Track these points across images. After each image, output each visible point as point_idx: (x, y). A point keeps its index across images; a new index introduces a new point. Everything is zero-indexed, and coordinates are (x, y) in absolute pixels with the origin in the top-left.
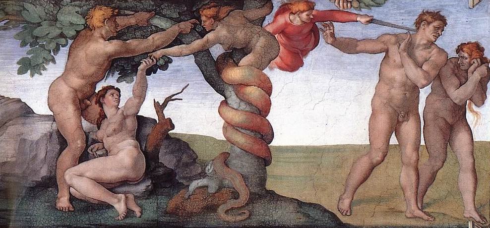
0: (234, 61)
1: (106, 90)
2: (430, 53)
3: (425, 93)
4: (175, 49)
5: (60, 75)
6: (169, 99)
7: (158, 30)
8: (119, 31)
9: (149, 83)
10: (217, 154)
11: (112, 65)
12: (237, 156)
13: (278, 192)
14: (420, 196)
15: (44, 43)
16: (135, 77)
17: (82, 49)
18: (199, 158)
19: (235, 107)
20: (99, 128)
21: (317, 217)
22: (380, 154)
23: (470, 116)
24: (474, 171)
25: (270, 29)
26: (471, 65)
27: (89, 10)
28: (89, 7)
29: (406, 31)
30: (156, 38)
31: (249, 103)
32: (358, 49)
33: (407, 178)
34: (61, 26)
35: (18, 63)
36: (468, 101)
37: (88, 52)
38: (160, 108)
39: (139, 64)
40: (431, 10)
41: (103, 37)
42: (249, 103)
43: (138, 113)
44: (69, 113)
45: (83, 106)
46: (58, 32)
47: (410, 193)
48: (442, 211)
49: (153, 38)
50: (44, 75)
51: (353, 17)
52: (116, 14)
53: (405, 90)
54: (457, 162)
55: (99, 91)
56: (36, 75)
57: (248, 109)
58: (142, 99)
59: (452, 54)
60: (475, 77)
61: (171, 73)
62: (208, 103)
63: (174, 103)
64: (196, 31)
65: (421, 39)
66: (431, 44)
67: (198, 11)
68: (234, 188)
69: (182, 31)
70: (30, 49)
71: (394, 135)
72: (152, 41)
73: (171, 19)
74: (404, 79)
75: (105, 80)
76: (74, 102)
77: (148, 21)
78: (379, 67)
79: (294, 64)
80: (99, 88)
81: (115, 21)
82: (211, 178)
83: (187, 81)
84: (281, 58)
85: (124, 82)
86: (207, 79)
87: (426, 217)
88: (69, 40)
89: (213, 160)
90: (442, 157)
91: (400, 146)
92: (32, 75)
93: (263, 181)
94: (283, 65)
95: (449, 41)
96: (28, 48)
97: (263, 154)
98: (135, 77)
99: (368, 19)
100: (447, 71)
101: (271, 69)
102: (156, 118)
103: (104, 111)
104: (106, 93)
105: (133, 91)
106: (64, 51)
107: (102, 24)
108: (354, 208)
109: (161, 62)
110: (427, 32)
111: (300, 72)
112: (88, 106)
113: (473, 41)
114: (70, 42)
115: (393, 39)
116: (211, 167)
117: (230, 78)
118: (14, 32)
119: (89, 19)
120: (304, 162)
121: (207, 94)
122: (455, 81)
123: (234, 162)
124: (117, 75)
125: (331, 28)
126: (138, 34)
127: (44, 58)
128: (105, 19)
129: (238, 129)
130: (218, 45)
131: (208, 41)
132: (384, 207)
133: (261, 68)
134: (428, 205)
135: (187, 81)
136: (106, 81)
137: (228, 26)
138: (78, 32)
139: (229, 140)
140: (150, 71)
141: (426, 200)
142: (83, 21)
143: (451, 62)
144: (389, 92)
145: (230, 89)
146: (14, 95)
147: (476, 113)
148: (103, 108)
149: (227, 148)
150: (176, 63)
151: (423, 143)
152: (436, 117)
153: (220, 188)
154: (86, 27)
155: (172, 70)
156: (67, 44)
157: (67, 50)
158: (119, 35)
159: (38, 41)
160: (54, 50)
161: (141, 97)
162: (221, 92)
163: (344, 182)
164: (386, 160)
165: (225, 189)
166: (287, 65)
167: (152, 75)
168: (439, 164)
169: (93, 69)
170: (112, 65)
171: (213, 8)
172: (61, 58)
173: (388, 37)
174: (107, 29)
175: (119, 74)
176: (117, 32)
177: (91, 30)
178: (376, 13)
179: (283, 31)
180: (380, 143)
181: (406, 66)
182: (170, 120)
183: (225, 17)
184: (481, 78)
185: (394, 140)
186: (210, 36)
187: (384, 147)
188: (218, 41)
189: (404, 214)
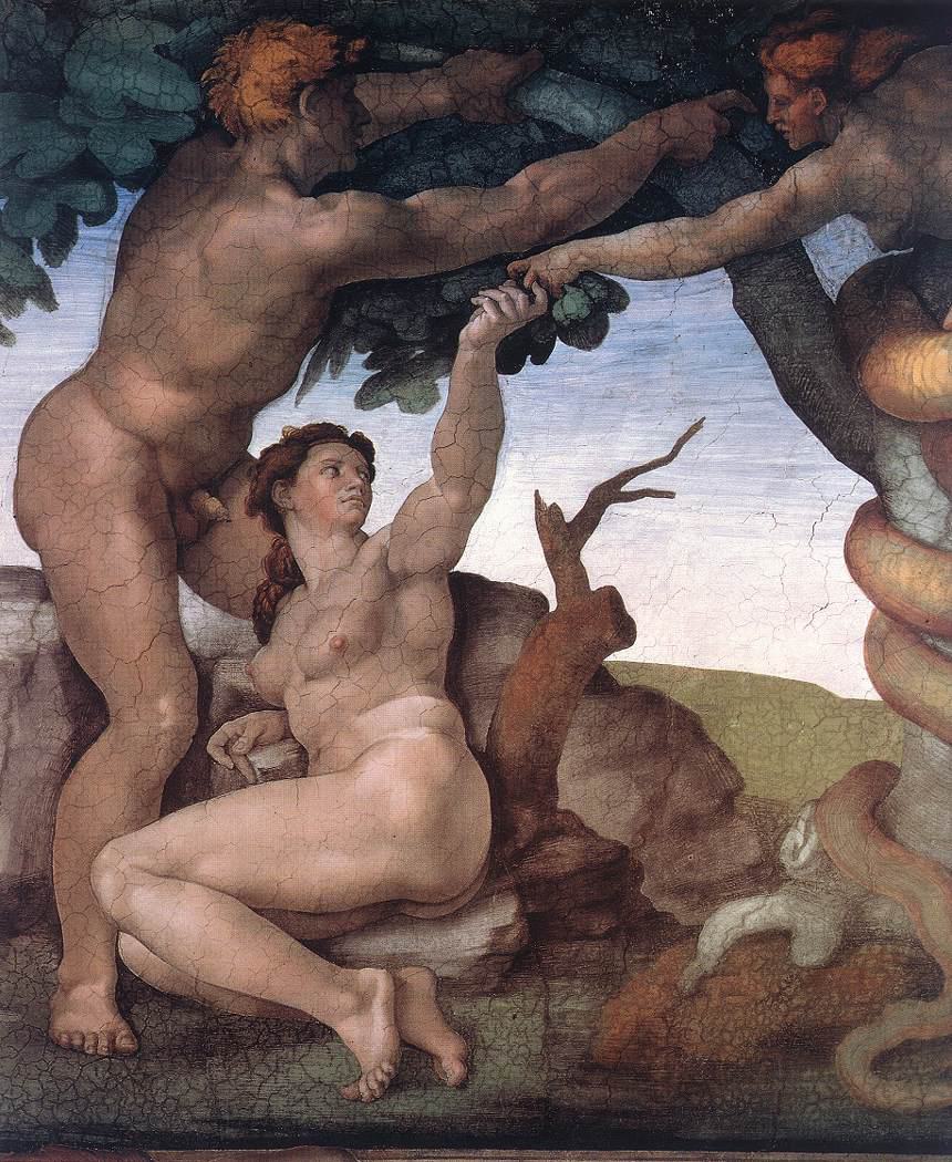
0: (922, 302)
1: (301, 443)
4: (639, 240)
6: (608, 494)
7: (559, 141)
8: (371, 147)
9: (512, 411)
10: (835, 768)
11: (334, 318)
16: (443, 383)
17: (187, 234)
18: (748, 792)
19: (927, 532)
20: (264, 630)
27: (218, 38)
28: (218, 21)
34: (87, 122)
37: (211, 252)
39: (465, 312)
45: (188, 523)
49: (534, 185)
52: (353, 59)
55: (266, 452)
58: (476, 491)
61: (620, 363)
63: (635, 512)
64: (742, 148)
68: (917, 944)
69: (674, 150)
72: (527, 200)
75: (301, 393)
76: (142, 501)
77: (510, 94)
80: (266, 433)
81: (350, 100)
82: (805, 889)
83: (694, 403)
85: (393, 406)
86: (794, 395)
88: (122, 192)
89: (818, 801)
98: (443, 383)
102: (546, 585)
103: (289, 547)
105: (434, 452)
106: (96, 245)
107: (277, 113)
109: (572, 305)
112: (208, 525)
114: (127, 200)
116: (806, 840)
117: (904, 388)
119: (221, 87)
121: (793, 467)
124: (356, 370)
126: (461, 161)
128: (299, 87)
129: (939, 644)
130: (850, 220)
131: (795, 204)
135: (694, 403)
136: (306, 399)
137: (895, 125)
138: (165, 152)
142: (188, 96)
145: (906, 444)
148: (285, 535)
149: (887, 742)
150: (646, 307)
153: (852, 939)
155: (624, 347)
156: (111, 213)
157: (109, 240)
162: (860, 459)
165: (877, 948)
167: (529, 368)
170: (334, 318)
171: (824, 37)
175: (368, 365)
176: (358, 151)
177: (230, 141)
182: (612, 598)
183: (875, 83)
186: (807, 175)
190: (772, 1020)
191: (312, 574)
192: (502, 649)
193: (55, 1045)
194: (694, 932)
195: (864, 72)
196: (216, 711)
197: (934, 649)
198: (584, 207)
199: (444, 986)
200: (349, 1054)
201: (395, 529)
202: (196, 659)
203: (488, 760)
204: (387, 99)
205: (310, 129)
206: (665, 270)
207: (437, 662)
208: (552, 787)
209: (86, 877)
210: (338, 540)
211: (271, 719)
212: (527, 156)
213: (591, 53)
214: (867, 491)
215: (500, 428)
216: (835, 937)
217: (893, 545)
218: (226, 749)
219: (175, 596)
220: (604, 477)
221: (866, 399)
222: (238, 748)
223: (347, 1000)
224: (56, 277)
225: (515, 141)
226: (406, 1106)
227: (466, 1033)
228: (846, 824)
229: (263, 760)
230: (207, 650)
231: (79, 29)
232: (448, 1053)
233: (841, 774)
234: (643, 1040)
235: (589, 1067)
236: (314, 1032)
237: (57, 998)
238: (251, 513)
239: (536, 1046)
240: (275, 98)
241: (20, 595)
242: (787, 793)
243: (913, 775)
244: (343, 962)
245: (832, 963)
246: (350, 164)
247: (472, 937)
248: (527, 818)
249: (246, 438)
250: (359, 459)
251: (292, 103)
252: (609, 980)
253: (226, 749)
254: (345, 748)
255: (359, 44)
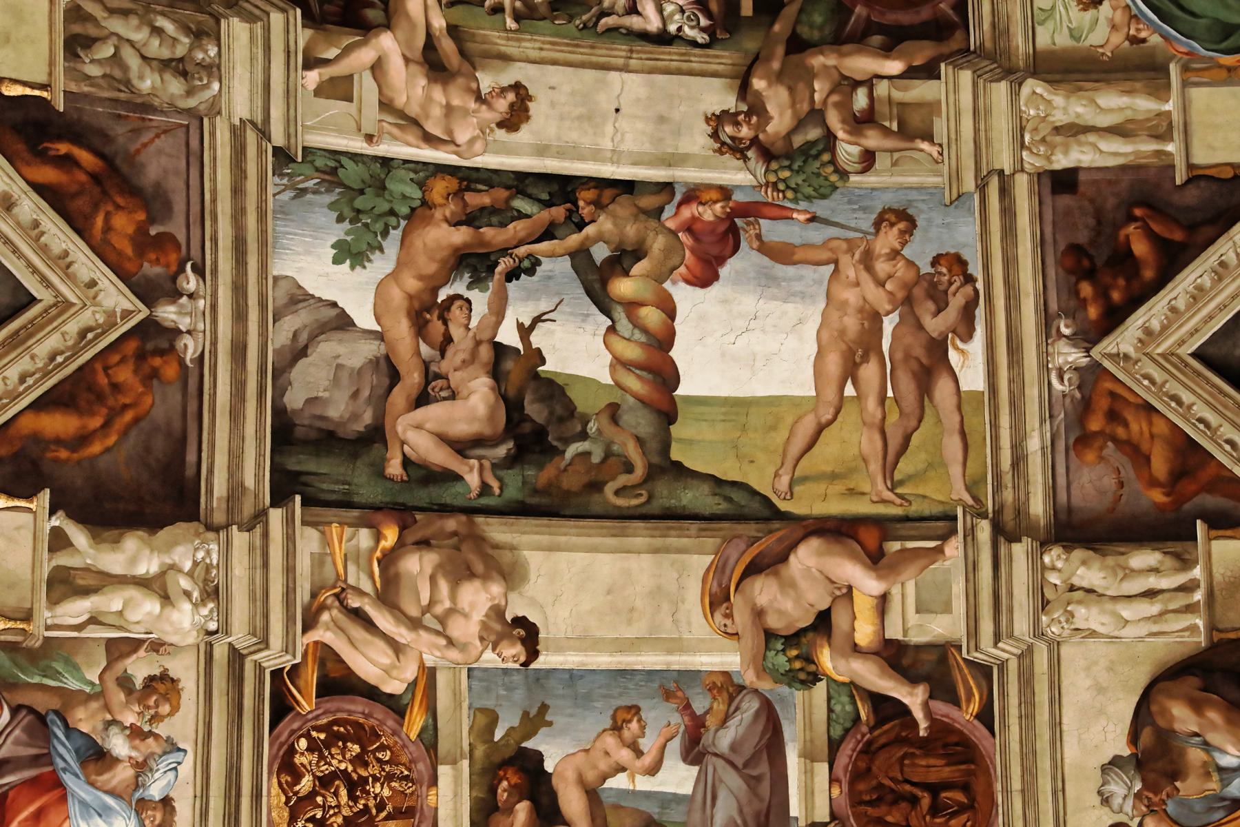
2: (895, 266)
3: (890, 323)
4: (545, 246)
5: (389, 271)
6: (537, 320)
7: (521, 216)
10: (602, 404)
12: (631, 409)
13: (688, 464)
14: (889, 469)
15: (369, 221)
16: (491, 284)
18: (578, 410)
19: (627, 337)
20: (443, 356)
21: (743, 503)
22: (832, 411)
23: (953, 356)
24: (963, 435)
25: (671, 224)
26: (951, 284)
28: (427, 174)
29: (861, 235)
30: (518, 228)
31: (645, 331)
32: (796, 257)
33: (870, 443)
35: (333, 247)
36: (950, 335)
38: (525, 332)
39: (496, 264)
40: (895, 206)
41: (447, 220)
42: (645, 331)
43: (495, 337)
44: (402, 329)
46: (385, 207)
47: (875, 467)
48: (921, 491)
49: (515, 228)
50: (368, 270)
51: (788, 214)
53: (863, 319)
54: (939, 421)
56: (358, 268)
57: (643, 339)
58: (500, 318)
59: (926, 269)
60: (956, 302)
62: (589, 328)
65: (882, 248)
66: (895, 254)
67: (574, 192)
68: (626, 457)
70: (350, 227)
71: (849, 383)
73: (539, 201)
74: (861, 302)
76: (409, 314)
77: (508, 200)
78: (826, 283)
79: (705, 278)
81: (463, 198)
82: (594, 440)
84: (687, 267)
86: (589, 293)
87: (898, 501)
88: (402, 221)
90: (917, 412)
91: (859, 397)
92: (352, 267)
93: (665, 446)
94: (694, 280)
95: (921, 251)
96: (346, 225)
97: (665, 406)
98: (491, 284)
99: (808, 216)
100: (918, 292)
101: (674, 283)
102: (520, 347)
104: (452, 304)
106: (396, 234)
107: (444, 201)
108: (797, 489)
109: (526, 264)
110: (889, 239)
111: (715, 290)
112: (427, 322)
113: (952, 251)
114: (403, 223)
115: (844, 246)
118: (328, 199)
120: (724, 421)
122: (931, 306)
123: (627, 418)
125: (757, 227)
126: (494, 220)
127: (368, 243)
128: (449, 195)
130: (601, 243)
131: (587, 238)
132: (839, 487)
133: (660, 280)
134: (901, 483)
138: (413, 210)
139: (618, 384)
140: (512, 275)
141: (898, 476)
143: (925, 280)
144: (841, 321)
146: (327, 295)
147: (962, 352)
150: (546, 266)
151: (890, 394)
152: (907, 357)
153: (608, 454)
154: (425, 203)
158: (470, 219)
159: (360, 216)
160: (381, 233)
161: (498, 311)
162: (606, 312)
163: (781, 450)
164: (840, 418)
166: (695, 277)
167: (514, 281)
168: (914, 423)
169: (431, 268)
172: (392, 244)
173: (835, 244)
174: (451, 208)
175: (470, 277)
177: (431, 209)
178: (821, 208)
179: (689, 228)
180: (830, 394)
181: (862, 283)
182: (539, 351)
184: (967, 303)
185: (849, 390)
186: (590, 230)
187: (837, 399)
188: (600, 238)
189: (868, 497)
190: (585, 479)
191: (455, 339)
192: (509, 365)
193: (384, 477)
194: (564, 452)
195: (605, 200)
196: (430, 378)
197: (629, 369)
198: (529, 235)
199: (495, 466)
200: (467, 485)
201: (478, 327)
202: (424, 362)
203: (504, 398)
204: (474, 200)
205: (452, 207)
206: (552, 255)
207: (490, 367)
208: (523, 407)
209: (394, 427)
210: (462, 329)
211: (444, 381)
212: (513, 219)
213: (531, 190)
214: (609, 323)
215: (507, 298)
216: (603, 455)
217: (618, 339)
218: (433, 390)
219: (418, 345)
220: (536, 315)
221: (609, 297)
222: (436, 390)
223: (467, 469)
224: (384, 244)
225: (510, 214)
226: (484, 501)
227: (500, 479)
228: (605, 420)
229: (444, 394)
230: (427, 360)
231: (389, 171)
232: (495, 485)
233: (603, 406)
234: (550, 484)
235: (536, 492)
236: (458, 478)
237: (386, 464)
238: (439, 319)
239: (520, 484)
240: (442, 197)
241: (375, 339)
242: (589, 411)
243: (624, 407)
244: (466, 457)
245: (604, 461)
246: (464, 218)
247: (502, 451)
248: (516, 416)
249: (436, 296)
250: (467, 305)
251: (447, 199)
252: (541, 467)
253: (433, 390)
254: (464, 393)
255: (465, 183)
